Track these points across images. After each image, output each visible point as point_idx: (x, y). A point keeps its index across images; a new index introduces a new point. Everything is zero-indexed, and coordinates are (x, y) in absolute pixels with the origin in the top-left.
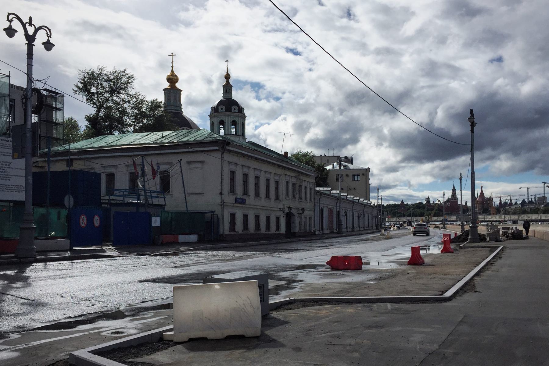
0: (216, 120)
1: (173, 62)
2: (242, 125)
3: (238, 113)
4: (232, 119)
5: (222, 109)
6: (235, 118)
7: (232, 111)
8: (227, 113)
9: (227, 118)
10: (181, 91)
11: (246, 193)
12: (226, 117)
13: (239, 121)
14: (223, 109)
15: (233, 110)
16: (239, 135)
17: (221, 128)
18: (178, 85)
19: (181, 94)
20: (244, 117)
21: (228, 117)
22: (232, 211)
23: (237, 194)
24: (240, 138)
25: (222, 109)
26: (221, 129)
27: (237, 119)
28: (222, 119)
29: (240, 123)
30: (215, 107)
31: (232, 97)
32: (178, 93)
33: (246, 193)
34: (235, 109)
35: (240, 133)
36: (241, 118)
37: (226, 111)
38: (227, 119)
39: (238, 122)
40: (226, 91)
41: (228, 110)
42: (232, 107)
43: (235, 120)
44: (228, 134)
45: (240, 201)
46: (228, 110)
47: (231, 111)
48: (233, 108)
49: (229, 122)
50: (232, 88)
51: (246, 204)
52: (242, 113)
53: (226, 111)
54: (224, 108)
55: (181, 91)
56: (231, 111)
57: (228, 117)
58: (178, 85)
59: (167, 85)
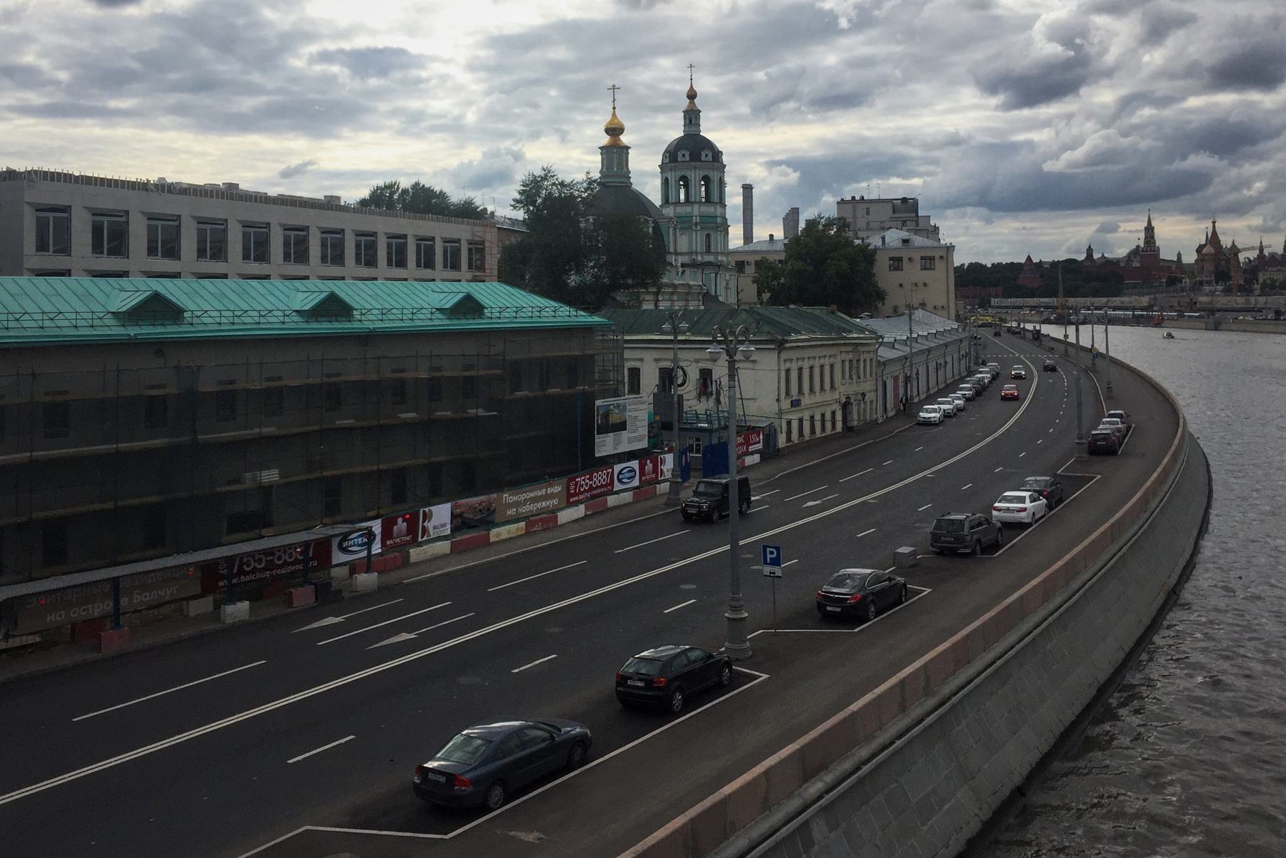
0: (672, 176)
1: (614, 100)
5: (684, 156)
7: (703, 159)
8: (693, 164)
9: (693, 171)
13: (714, 176)
16: (713, 202)
18: (625, 139)
19: (628, 153)
21: (695, 171)
23: (792, 396)
24: (716, 208)
25: (684, 156)
27: (711, 174)
28: (683, 173)
29: (716, 180)
30: (672, 152)
34: (706, 156)
37: (691, 160)
38: (693, 175)
39: (712, 179)
41: (695, 157)
42: (702, 153)
43: (709, 175)
44: (696, 202)
45: (796, 404)
46: (695, 157)
53: (691, 160)
56: (700, 160)
57: (695, 171)
58: (625, 139)
59: (605, 140)
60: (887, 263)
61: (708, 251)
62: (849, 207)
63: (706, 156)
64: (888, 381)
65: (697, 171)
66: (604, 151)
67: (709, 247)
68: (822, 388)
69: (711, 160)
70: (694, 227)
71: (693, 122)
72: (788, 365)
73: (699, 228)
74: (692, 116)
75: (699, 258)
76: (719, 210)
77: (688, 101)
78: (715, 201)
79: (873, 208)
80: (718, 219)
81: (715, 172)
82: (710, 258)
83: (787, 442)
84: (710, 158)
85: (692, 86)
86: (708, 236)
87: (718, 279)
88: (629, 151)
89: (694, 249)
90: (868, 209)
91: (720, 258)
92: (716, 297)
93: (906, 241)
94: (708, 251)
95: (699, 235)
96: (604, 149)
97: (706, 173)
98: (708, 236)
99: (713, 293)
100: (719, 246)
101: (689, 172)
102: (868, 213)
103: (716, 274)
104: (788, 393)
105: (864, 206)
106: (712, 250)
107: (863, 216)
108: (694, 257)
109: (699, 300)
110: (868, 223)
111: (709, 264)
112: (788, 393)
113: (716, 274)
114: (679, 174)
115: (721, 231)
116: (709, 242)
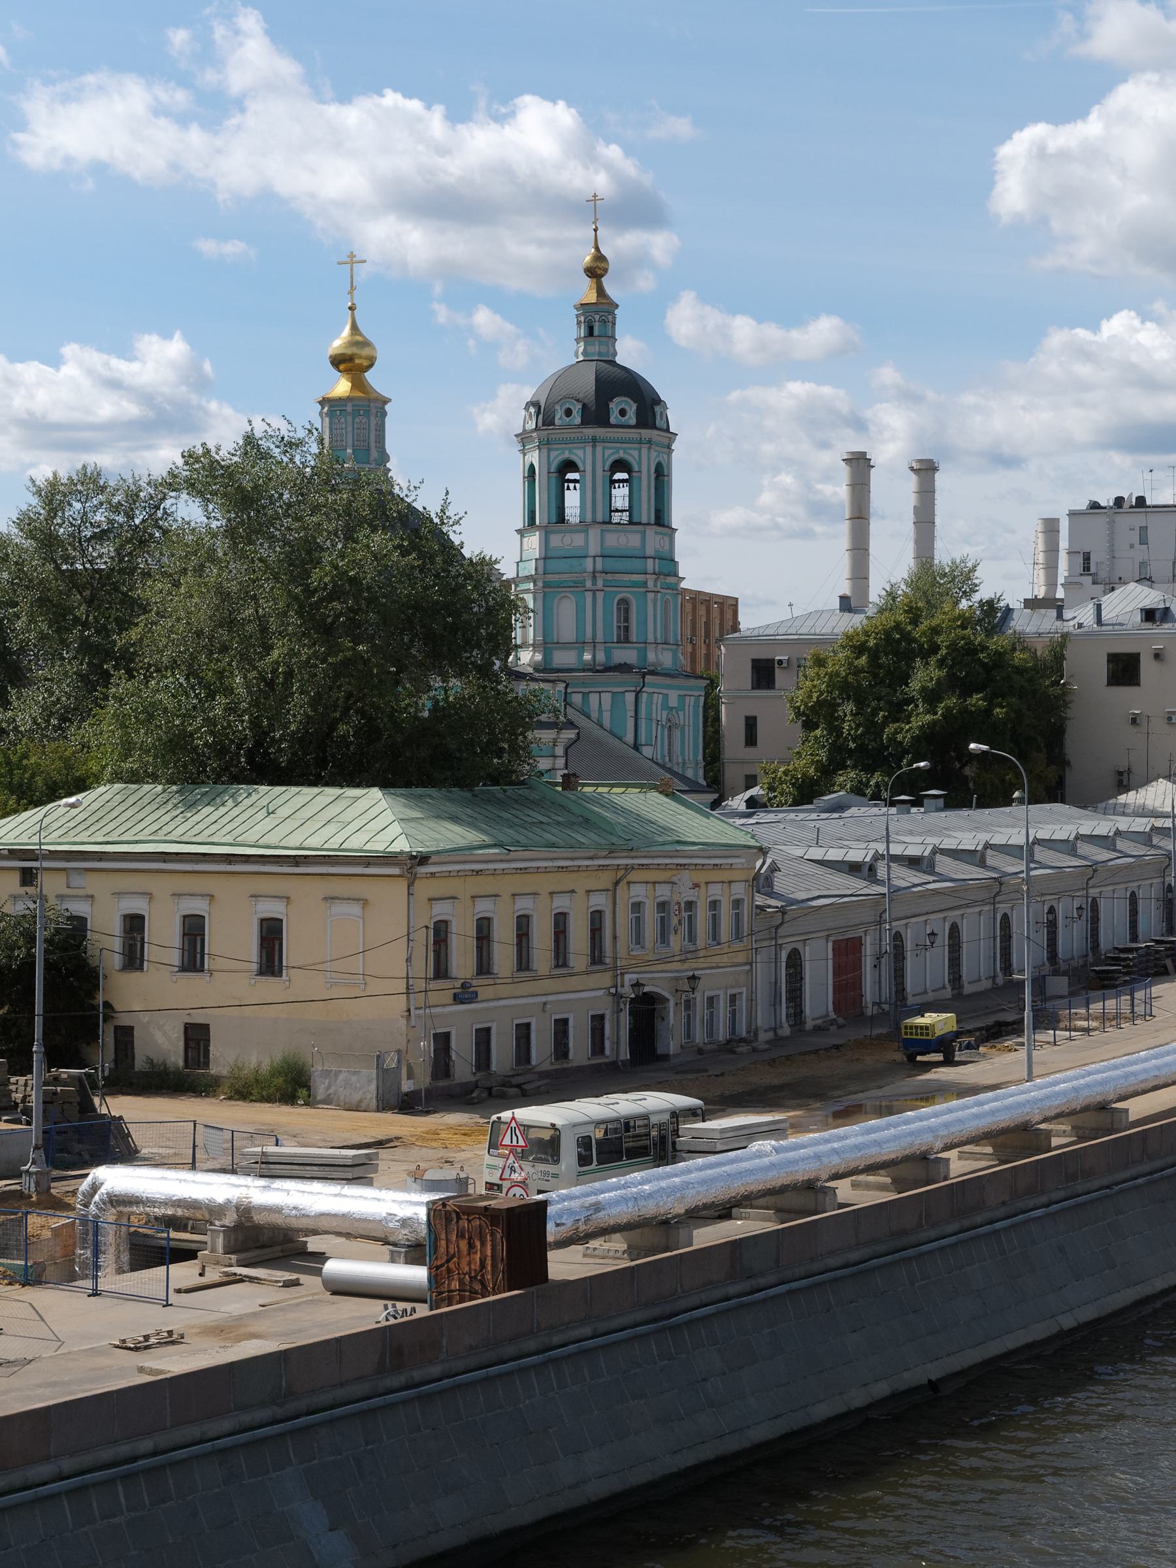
2: (657, 478)
3: (637, 426)
4: (610, 455)
6: (624, 449)
7: (612, 420)
8: (590, 432)
9: (589, 449)
10: (386, 401)
11: (484, 967)
12: (584, 448)
14: (574, 412)
16: (640, 523)
17: (570, 481)
19: (385, 414)
21: (594, 447)
24: (644, 534)
26: (572, 485)
27: (631, 456)
28: (566, 455)
31: (615, 354)
32: (374, 411)
33: (484, 967)
34: (623, 413)
35: (646, 513)
36: (649, 448)
37: (585, 422)
40: (590, 332)
42: (611, 405)
45: (464, 995)
48: (615, 406)
50: (614, 318)
51: (479, 999)
52: (654, 427)
53: (585, 422)
54: (577, 408)
55: (386, 401)
57: (594, 447)
60: (1101, 669)
62: (1100, 521)
63: (622, 407)
64: (807, 953)
65: (599, 449)
66: (326, 409)
67: (627, 629)
68: (523, 963)
69: (633, 421)
70: (589, 584)
71: (596, 332)
72: (442, 910)
73: (600, 583)
77: (587, 283)
78: (644, 520)
79: (1156, 524)
81: (644, 451)
84: (631, 417)
88: (387, 407)
90: (1144, 530)
91: (651, 657)
93: (1149, 615)
94: (624, 637)
97: (621, 455)
101: (580, 452)
102: (1143, 541)
103: (638, 694)
104: (441, 971)
105: (1138, 520)
107: (1132, 546)
110: (1143, 564)
111: (624, 668)
112: (441, 971)
113: (638, 694)
114: (558, 456)
116: (627, 620)
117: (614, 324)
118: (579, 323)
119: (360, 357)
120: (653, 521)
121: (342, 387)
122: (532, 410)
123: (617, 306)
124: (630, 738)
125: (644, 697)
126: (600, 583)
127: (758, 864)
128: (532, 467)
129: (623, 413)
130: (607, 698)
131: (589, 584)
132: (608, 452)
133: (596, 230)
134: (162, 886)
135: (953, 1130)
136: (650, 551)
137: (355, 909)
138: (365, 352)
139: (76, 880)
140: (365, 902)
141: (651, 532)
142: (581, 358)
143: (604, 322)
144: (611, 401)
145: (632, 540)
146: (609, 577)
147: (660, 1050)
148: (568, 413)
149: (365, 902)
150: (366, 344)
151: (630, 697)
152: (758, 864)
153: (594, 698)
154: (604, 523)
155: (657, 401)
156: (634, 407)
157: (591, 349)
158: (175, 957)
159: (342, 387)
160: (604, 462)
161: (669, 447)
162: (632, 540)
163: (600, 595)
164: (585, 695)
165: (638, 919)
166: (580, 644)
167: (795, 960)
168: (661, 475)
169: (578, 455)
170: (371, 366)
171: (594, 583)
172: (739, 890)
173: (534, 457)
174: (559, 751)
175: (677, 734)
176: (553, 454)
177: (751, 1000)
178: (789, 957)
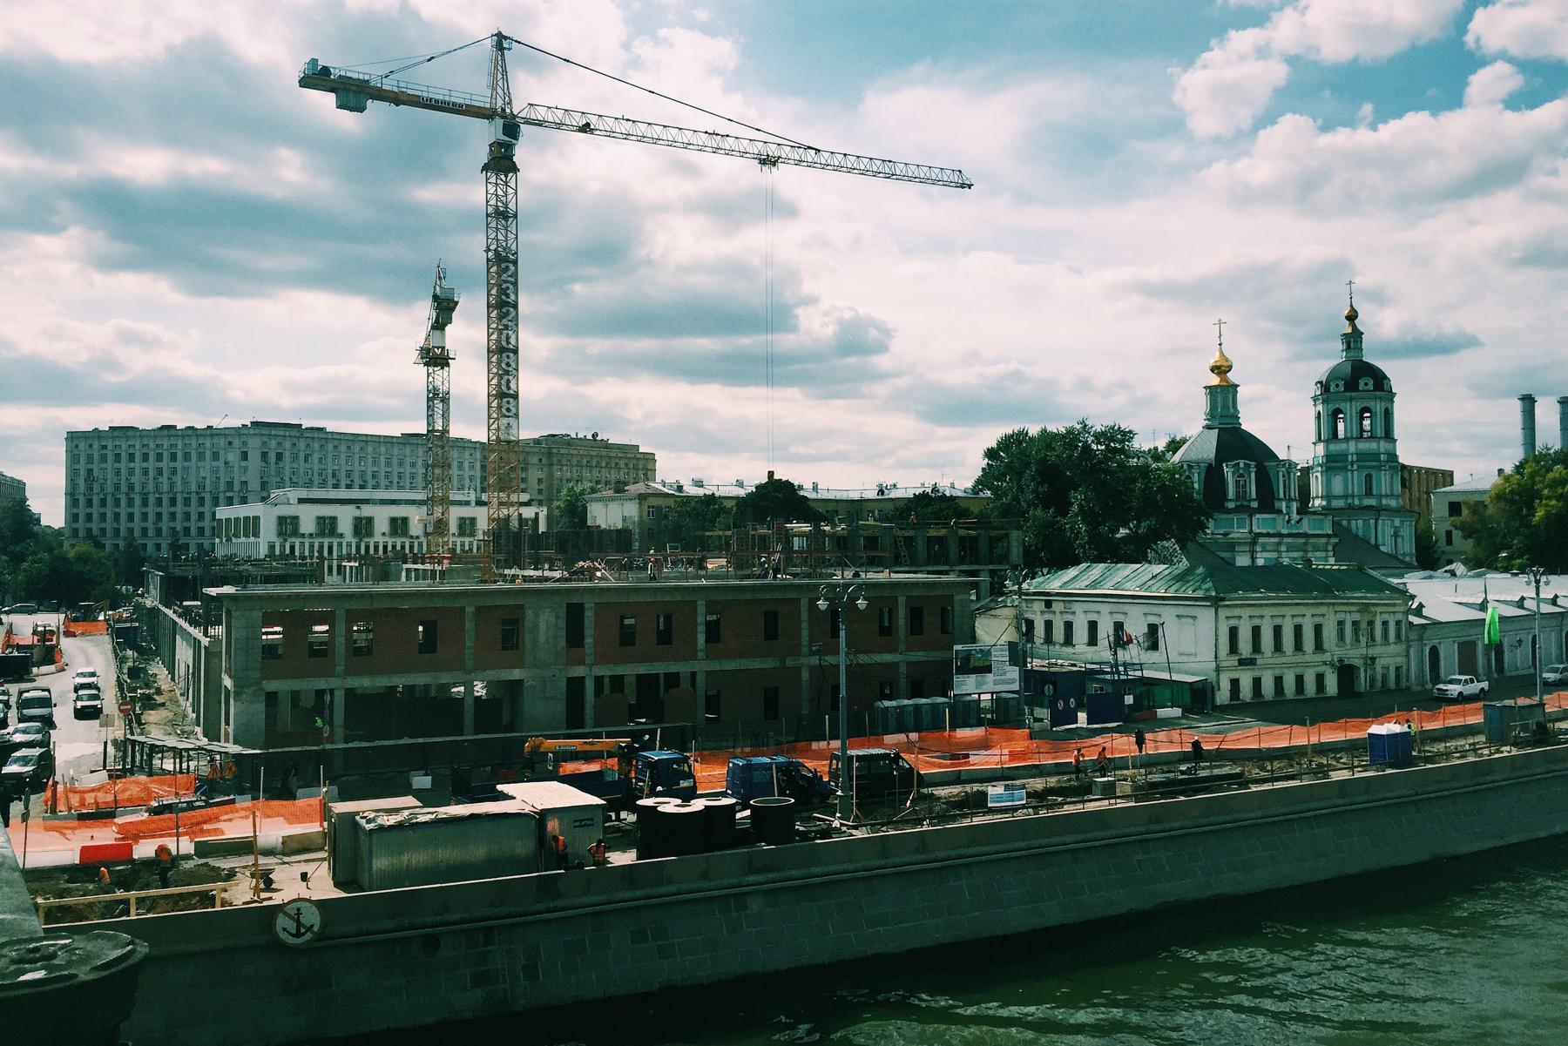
3: (1374, 390)
7: (1360, 388)
9: (1348, 403)
13: (1378, 407)
15: (1361, 387)
18: (1232, 376)
20: (1390, 396)
22: (1234, 675)
23: (1241, 654)
27: (1371, 404)
28: (1337, 406)
29: (1378, 413)
31: (1362, 356)
34: (1366, 384)
35: (1380, 432)
37: (1346, 390)
40: (1349, 347)
43: (1368, 405)
47: (1356, 389)
49: (1354, 414)
50: (1362, 339)
53: (1346, 390)
54: (1341, 384)
58: (1232, 376)
61: (1369, 493)
63: (1366, 383)
65: (1354, 403)
67: (1371, 489)
70: (1349, 467)
71: (1352, 346)
73: (1355, 467)
74: (1353, 339)
75: (1357, 502)
76: (1384, 446)
80: (1382, 456)
81: (1378, 402)
82: (1372, 502)
83: (1231, 700)
85: (1351, 306)
86: (1369, 478)
87: (1380, 527)
89: (1350, 492)
92: (1377, 546)
94: (1369, 493)
95: (1356, 477)
96: (1211, 389)
98: (1369, 478)
99: (1373, 541)
100: (1383, 489)
106: (1375, 493)
108: (1350, 501)
109: (1327, 551)
111: (1369, 508)
114: (1332, 407)
115: (1386, 470)
117: (1361, 342)
118: (1343, 343)
119: (1224, 366)
120: (1383, 435)
121: (1215, 380)
122: (1319, 385)
123: (1363, 334)
124: (1373, 541)
125: (1380, 522)
126: (1355, 467)
127: (1410, 603)
128: (1319, 412)
129: (1366, 384)
130: (1360, 522)
131: (1349, 467)
132: (1358, 404)
133: (1351, 298)
134: (1105, 609)
135: (528, 636)
136: (1382, 450)
137: (1190, 620)
138: (1226, 364)
139: (1068, 605)
140: (1194, 618)
141: (1382, 443)
142: (1344, 359)
143: (1356, 341)
144: (1360, 378)
145: (1373, 446)
146: (1362, 464)
147: (1357, 690)
148: (1337, 386)
149: (1194, 618)
150: (1227, 360)
151: (1372, 522)
152: (1410, 603)
153: (1353, 522)
154: (1357, 438)
155: (1385, 377)
156: (1372, 382)
157: (1349, 355)
158: (1086, 639)
159: (1215, 380)
160: (1356, 410)
161: (1392, 399)
162: (1373, 446)
163: (1355, 472)
164: (1349, 522)
165: (1341, 629)
166: (1345, 497)
167: (1434, 652)
168: (1388, 415)
169: (1342, 406)
170: (1230, 370)
171: (1352, 467)
172: (1399, 617)
173: (1320, 407)
174: (1330, 548)
175: (1399, 540)
176: (1330, 406)
177: (1408, 669)
178: (1431, 649)
